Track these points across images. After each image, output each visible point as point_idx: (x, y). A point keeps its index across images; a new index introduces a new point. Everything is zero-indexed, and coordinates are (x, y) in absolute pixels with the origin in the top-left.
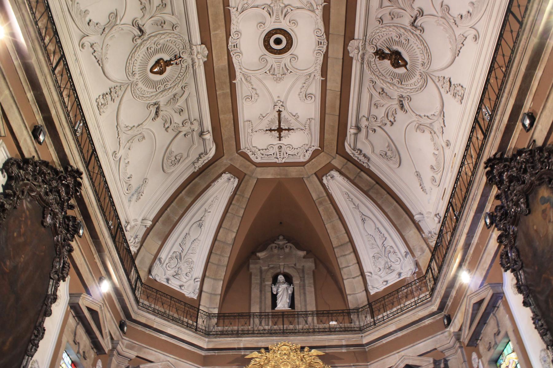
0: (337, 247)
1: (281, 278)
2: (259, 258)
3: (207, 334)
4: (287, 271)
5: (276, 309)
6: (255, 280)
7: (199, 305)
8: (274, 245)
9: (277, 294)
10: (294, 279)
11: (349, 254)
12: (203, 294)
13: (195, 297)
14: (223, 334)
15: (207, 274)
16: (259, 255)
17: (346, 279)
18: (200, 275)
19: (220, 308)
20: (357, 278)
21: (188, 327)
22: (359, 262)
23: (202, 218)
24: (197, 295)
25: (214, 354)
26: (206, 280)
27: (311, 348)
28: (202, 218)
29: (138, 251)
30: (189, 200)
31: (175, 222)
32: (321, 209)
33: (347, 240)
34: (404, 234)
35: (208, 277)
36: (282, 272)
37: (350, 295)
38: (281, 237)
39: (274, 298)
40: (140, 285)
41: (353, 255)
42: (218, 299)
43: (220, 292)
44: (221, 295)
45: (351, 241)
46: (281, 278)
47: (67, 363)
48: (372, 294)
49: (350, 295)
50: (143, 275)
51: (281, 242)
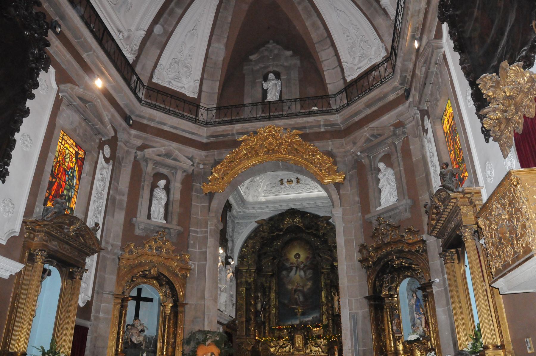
0: (316, 43)
1: (271, 76)
2: (251, 61)
3: (207, 124)
4: (276, 69)
5: (266, 101)
6: (248, 79)
7: (200, 102)
8: (263, 48)
9: (267, 89)
10: (281, 75)
11: (328, 48)
12: (203, 94)
13: (196, 97)
14: (219, 123)
15: (205, 76)
16: (251, 57)
17: (325, 71)
18: (199, 77)
19: (218, 104)
20: (336, 69)
21: (189, 119)
22: (337, 54)
23: (194, 27)
24: (197, 95)
25: (212, 140)
26: (204, 82)
27: (293, 129)
28: (194, 27)
29: (138, 58)
30: (179, 11)
31: (169, 32)
32: (300, 8)
33: (326, 35)
34: (374, 23)
35: (206, 79)
36: (272, 71)
37: (330, 84)
38: (271, 41)
39: (265, 93)
40: (141, 86)
41: (331, 48)
42: (216, 97)
43: (217, 91)
44: (218, 93)
45: (329, 36)
46: (271, 76)
47: (71, 144)
48: (348, 81)
49: (330, 84)
50: (145, 80)
51: (271, 45)
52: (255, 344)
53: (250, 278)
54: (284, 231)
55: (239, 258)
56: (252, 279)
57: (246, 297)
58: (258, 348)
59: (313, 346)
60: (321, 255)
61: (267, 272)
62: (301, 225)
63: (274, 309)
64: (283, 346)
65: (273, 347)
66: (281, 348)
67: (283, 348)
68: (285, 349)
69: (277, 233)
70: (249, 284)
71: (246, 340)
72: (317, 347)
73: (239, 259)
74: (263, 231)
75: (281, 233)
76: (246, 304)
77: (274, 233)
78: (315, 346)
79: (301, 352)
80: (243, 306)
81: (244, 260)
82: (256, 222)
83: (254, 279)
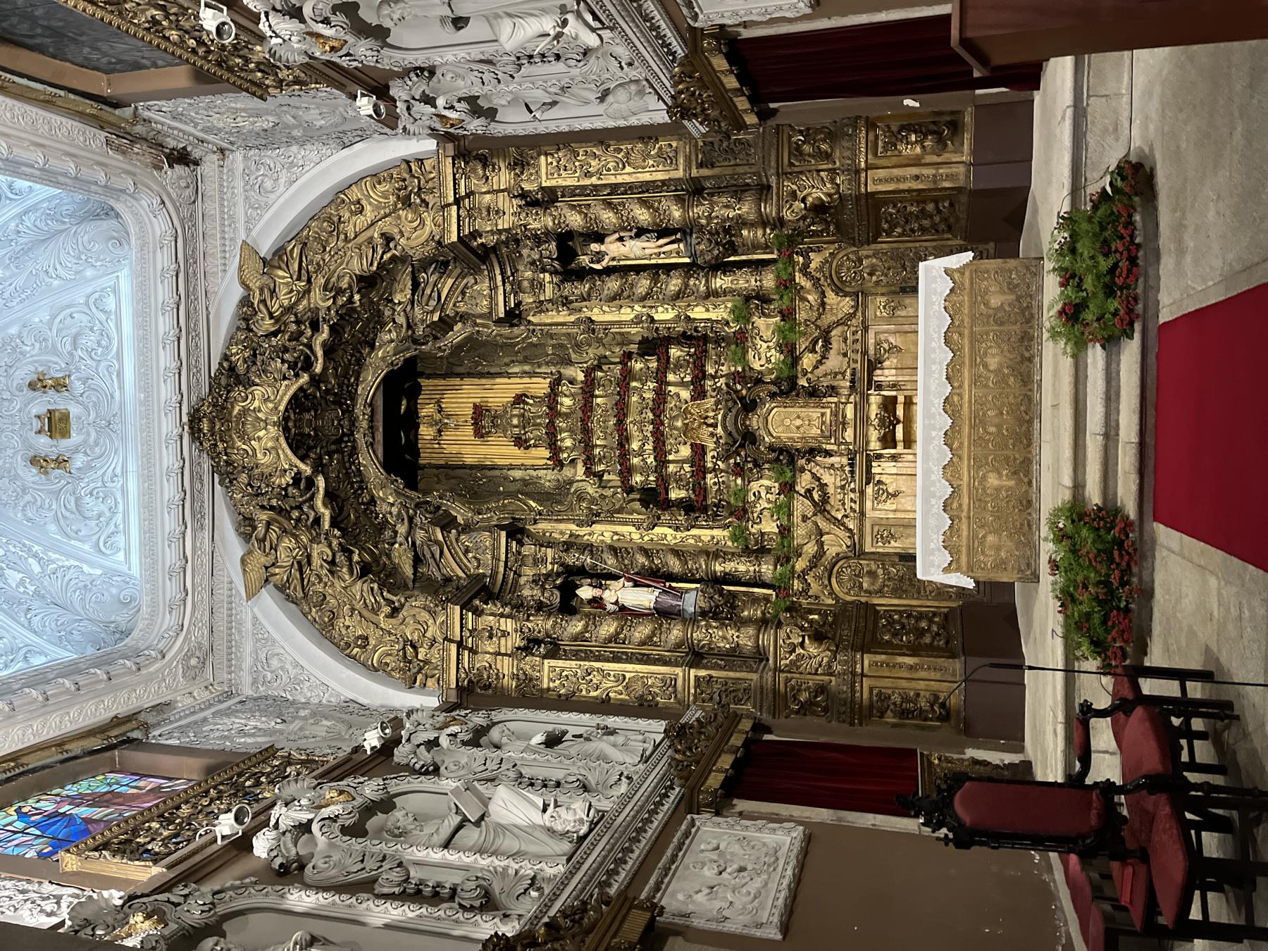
52: (802, 628)
53: (505, 634)
54: (307, 469)
55: (411, 684)
56: (508, 625)
57: (584, 660)
58: (824, 615)
59: (820, 362)
60: (436, 318)
61: (496, 558)
62: (288, 390)
63: (657, 530)
64: (816, 496)
65: (821, 544)
66: (828, 508)
67: (825, 498)
68: (831, 490)
69: (319, 502)
70: (531, 644)
71: (782, 671)
72: (827, 343)
73: (418, 683)
74: (304, 563)
75: (321, 482)
76: (616, 658)
77: (317, 521)
78: (824, 357)
79: (844, 417)
80: (628, 675)
81: (426, 662)
82: (249, 598)
83: (507, 617)
